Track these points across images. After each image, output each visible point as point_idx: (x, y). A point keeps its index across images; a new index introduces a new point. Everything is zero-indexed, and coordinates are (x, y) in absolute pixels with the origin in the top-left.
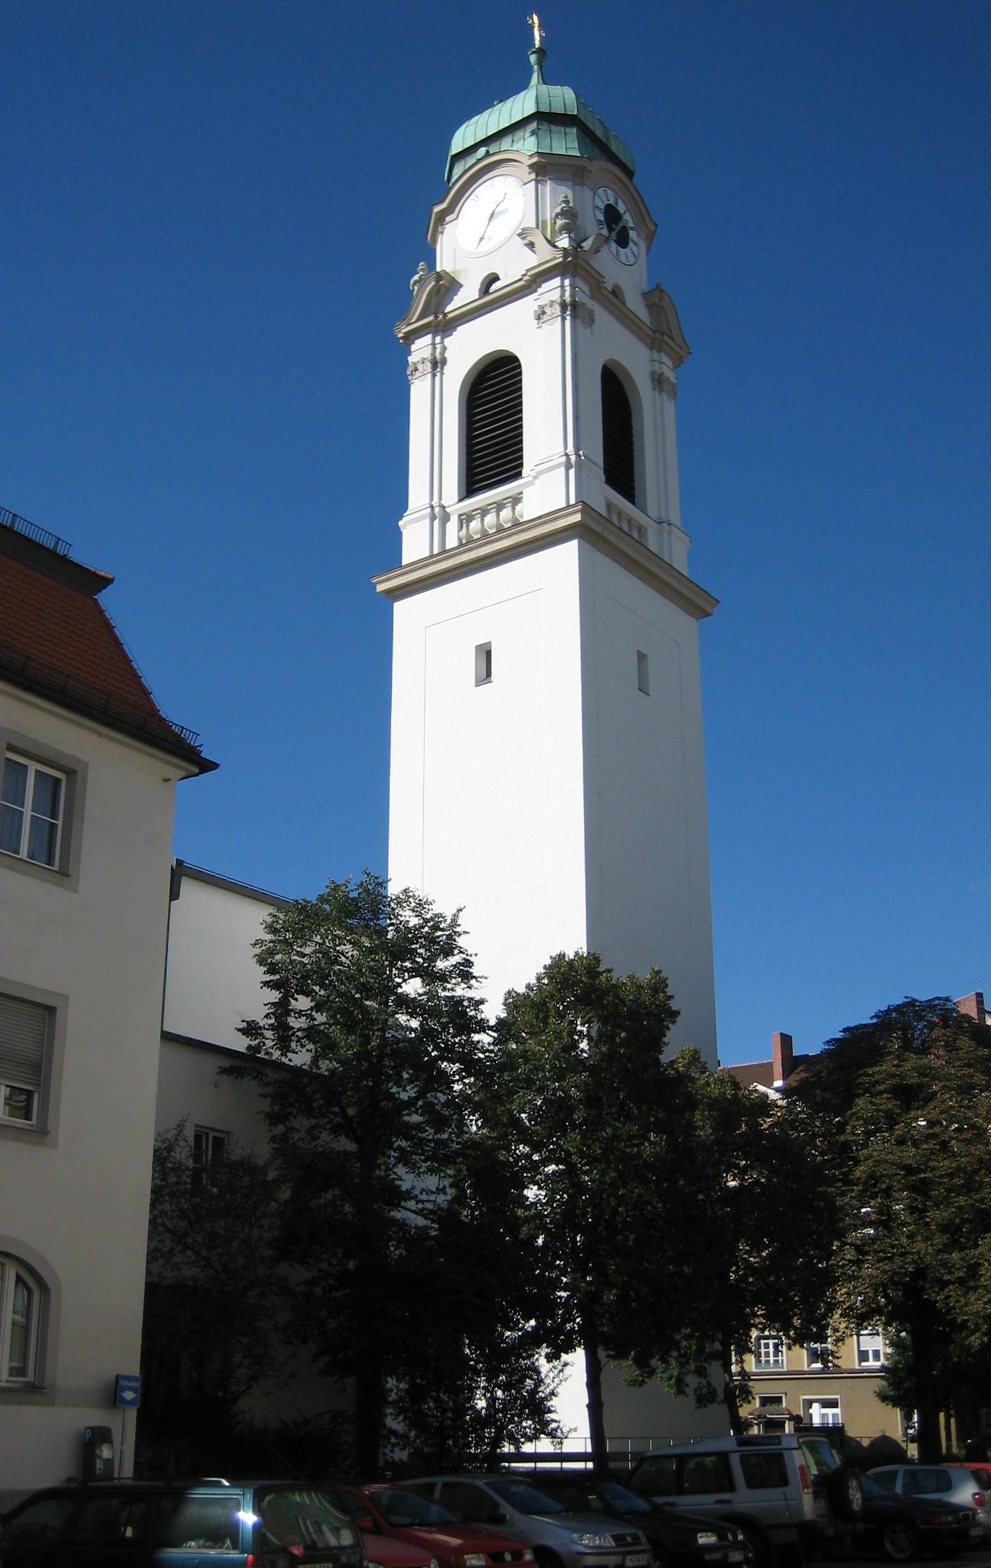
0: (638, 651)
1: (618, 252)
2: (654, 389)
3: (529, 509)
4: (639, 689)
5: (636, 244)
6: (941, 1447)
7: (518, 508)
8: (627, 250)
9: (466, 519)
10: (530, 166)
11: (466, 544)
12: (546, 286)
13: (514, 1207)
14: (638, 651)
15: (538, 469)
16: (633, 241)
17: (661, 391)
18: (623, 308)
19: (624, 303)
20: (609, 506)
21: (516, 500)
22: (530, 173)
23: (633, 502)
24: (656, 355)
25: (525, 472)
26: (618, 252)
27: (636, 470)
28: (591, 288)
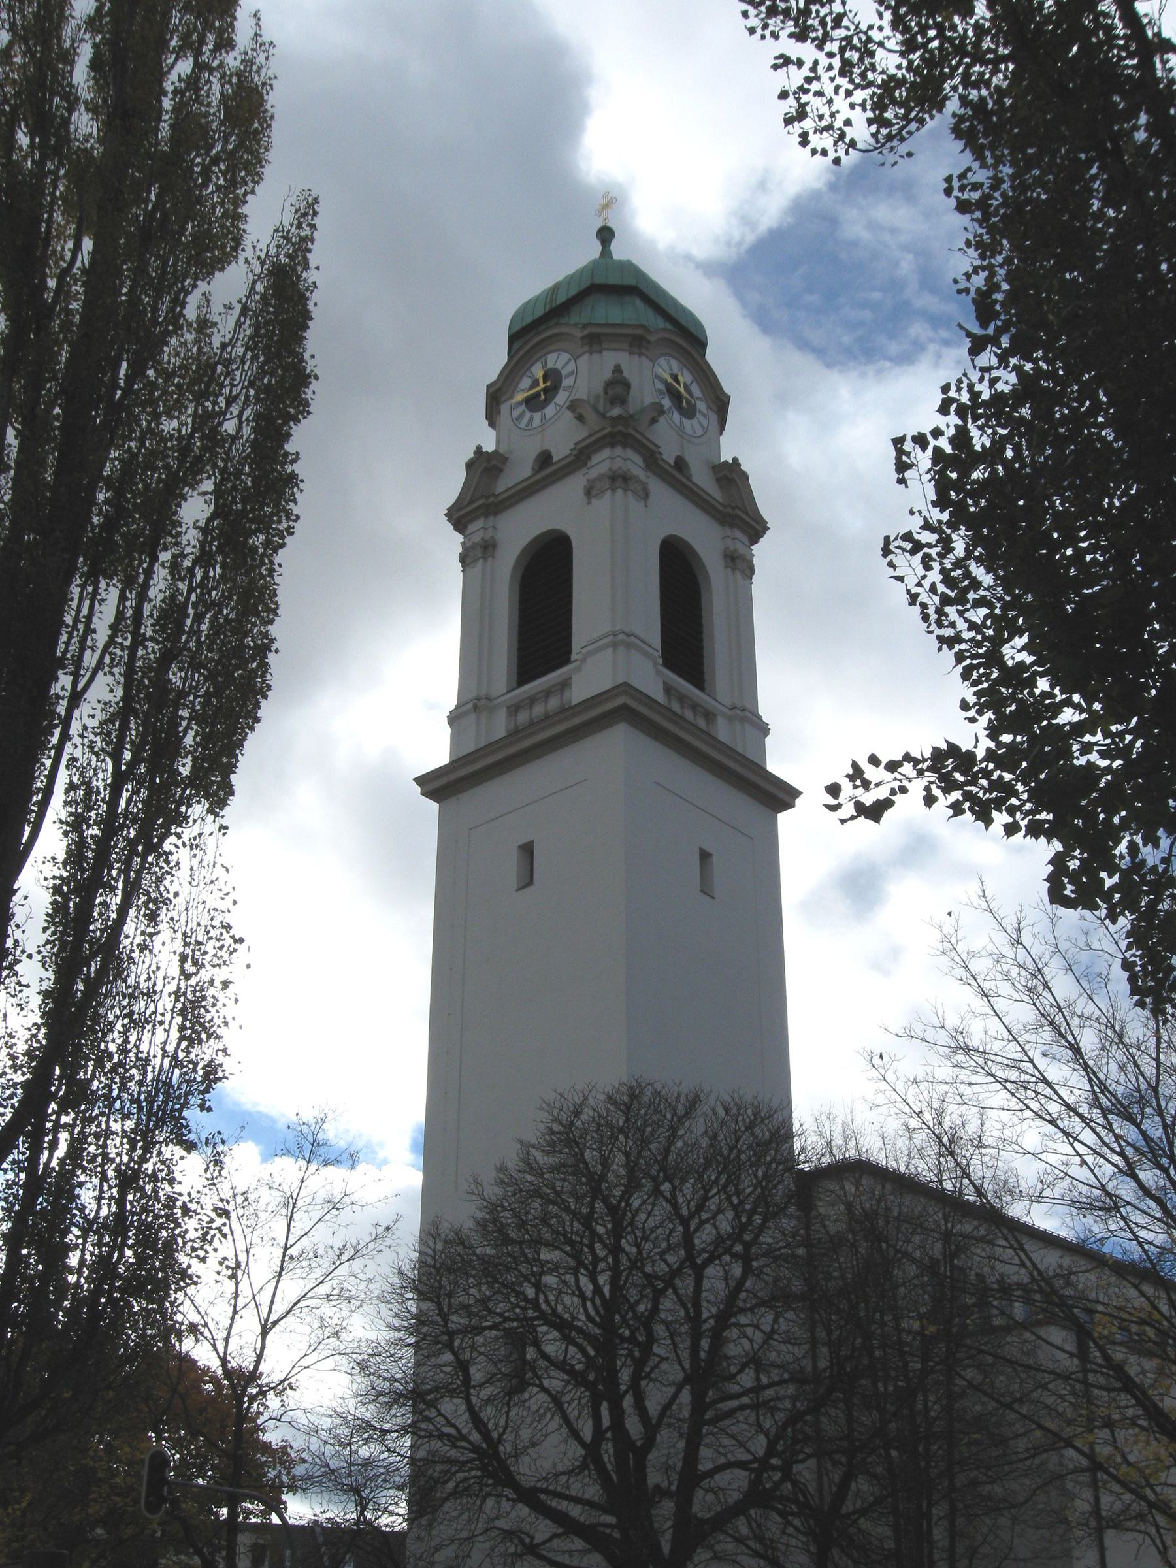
0: (701, 849)
1: (682, 423)
2: (726, 567)
3: (579, 693)
4: (702, 891)
5: (705, 416)
6: (23, 835)
7: (567, 695)
8: (694, 422)
9: (514, 709)
10: (583, 338)
11: (514, 734)
12: (596, 459)
13: (74, 1004)
14: (701, 849)
15: (584, 651)
16: (701, 412)
17: (734, 569)
18: (690, 484)
19: (689, 478)
20: (668, 689)
21: (565, 684)
22: (582, 346)
23: (702, 689)
24: (728, 531)
25: (573, 657)
26: (682, 423)
27: (706, 661)
28: (645, 460)
